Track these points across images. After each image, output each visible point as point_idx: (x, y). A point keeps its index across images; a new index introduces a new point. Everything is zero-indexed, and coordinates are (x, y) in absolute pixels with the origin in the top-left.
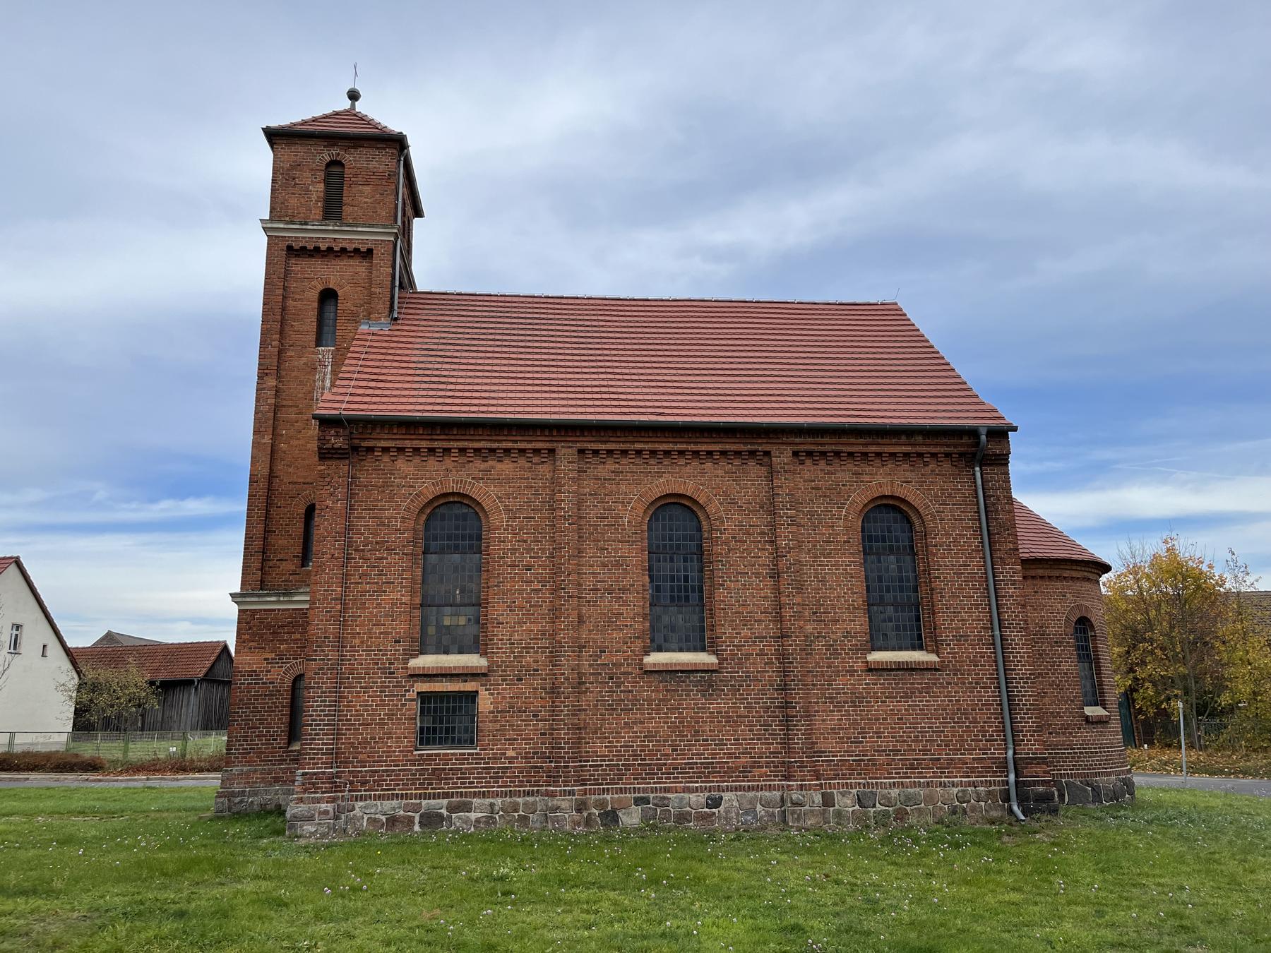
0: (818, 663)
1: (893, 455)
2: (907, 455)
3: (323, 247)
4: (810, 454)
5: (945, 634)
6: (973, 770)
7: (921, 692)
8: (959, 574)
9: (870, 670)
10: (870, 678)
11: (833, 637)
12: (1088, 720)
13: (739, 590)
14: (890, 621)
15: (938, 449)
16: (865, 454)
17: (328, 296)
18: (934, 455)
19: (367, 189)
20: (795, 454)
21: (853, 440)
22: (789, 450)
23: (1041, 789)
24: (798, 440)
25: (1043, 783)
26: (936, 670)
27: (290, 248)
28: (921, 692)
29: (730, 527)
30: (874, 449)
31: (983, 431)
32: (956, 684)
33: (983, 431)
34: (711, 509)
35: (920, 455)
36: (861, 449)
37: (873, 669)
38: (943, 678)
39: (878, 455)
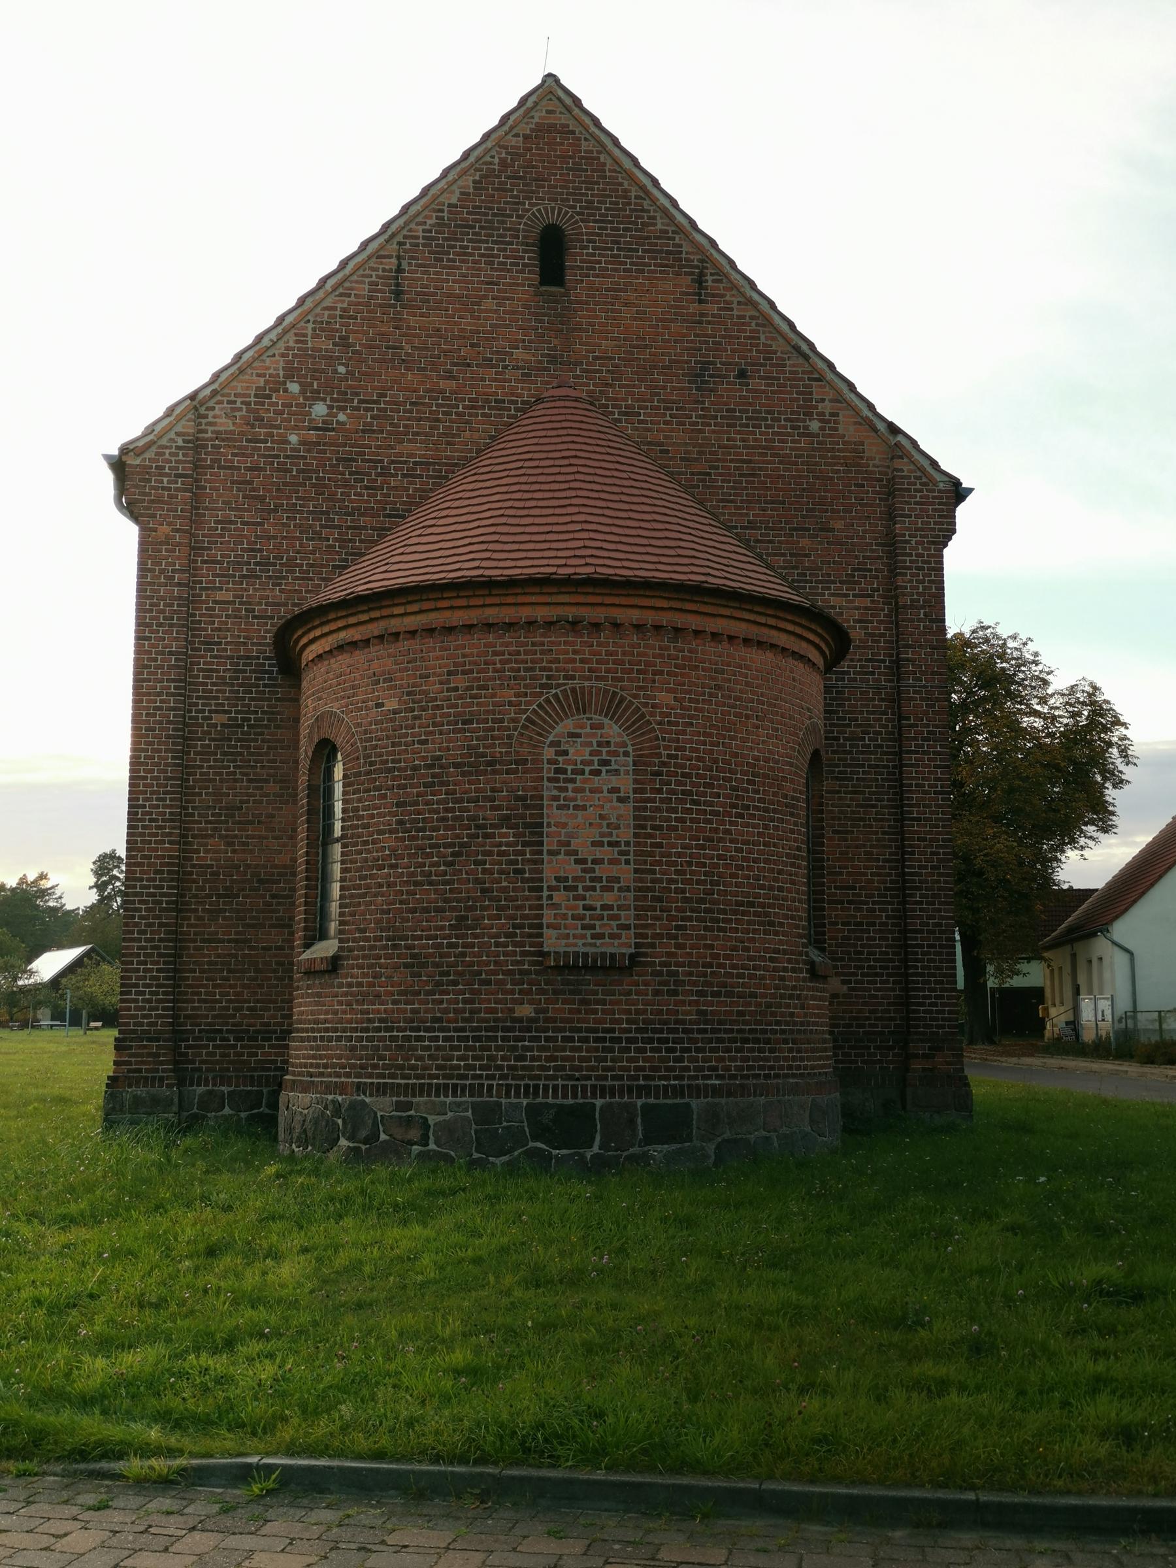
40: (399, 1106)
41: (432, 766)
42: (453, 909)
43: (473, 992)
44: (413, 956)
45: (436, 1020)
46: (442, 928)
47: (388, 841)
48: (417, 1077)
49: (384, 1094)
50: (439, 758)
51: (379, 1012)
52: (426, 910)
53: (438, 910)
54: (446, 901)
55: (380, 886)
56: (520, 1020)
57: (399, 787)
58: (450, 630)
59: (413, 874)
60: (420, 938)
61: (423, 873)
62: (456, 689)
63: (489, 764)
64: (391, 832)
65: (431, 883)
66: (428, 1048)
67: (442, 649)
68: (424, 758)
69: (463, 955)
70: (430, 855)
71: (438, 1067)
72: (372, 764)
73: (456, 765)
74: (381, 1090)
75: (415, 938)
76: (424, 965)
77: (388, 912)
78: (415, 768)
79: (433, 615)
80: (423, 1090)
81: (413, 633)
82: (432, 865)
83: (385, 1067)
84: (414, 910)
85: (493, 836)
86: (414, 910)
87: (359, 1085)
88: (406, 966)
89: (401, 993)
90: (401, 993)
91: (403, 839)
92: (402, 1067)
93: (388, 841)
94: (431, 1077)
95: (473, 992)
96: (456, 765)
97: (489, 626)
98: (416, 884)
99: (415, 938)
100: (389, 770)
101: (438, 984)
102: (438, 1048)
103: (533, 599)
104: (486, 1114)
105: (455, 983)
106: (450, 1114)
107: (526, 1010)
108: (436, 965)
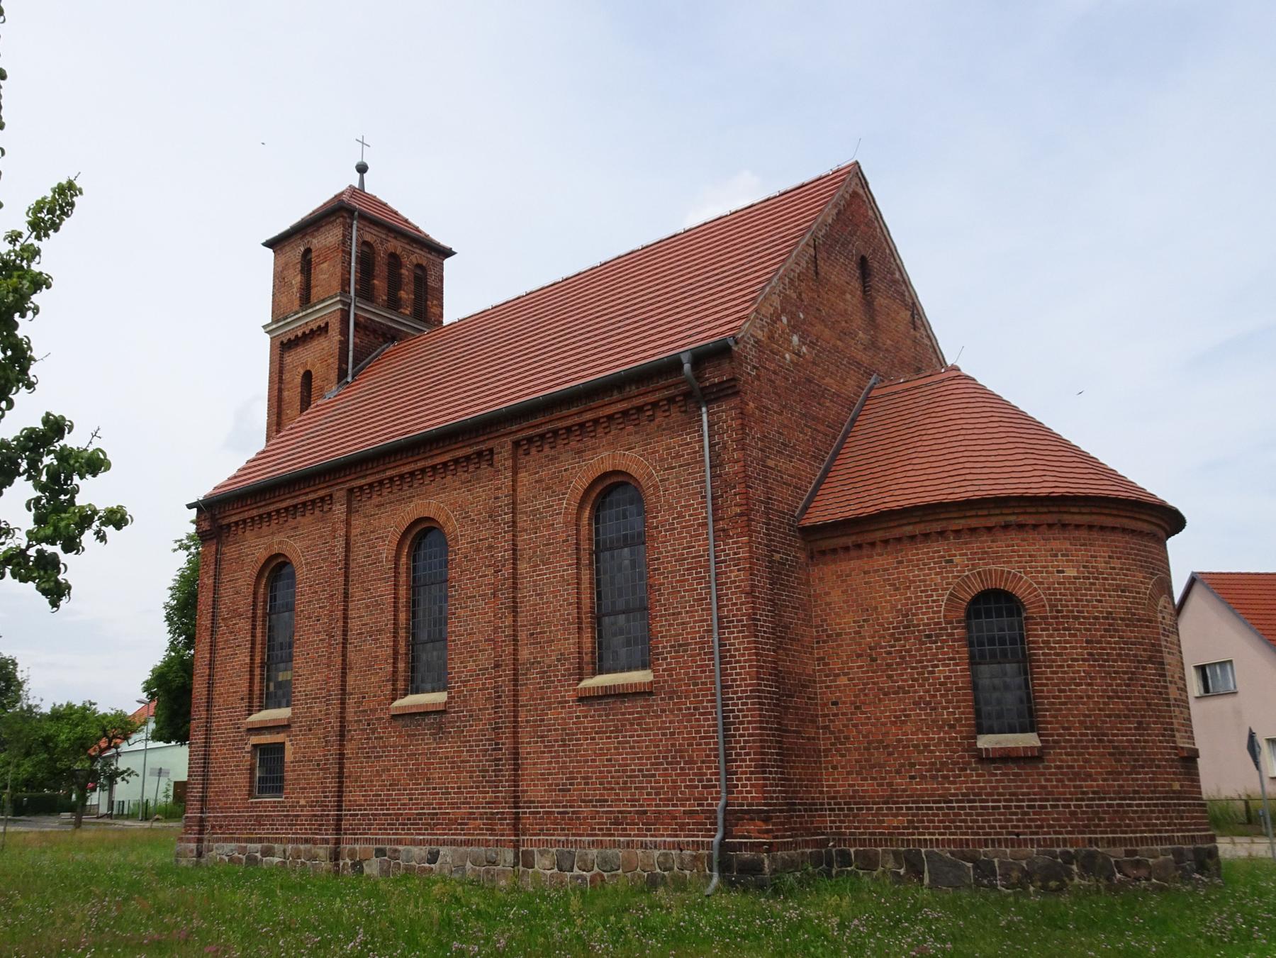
0: (532, 695)
1: (610, 418)
2: (625, 413)
3: (300, 334)
4: (530, 440)
5: (663, 645)
6: (682, 827)
7: (632, 724)
8: (681, 560)
9: (581, 699)
10: (580, 710)
11: (547, 661)
12: (986, 759)
13: (471, 617)
14: (621, 634)
15: (658, 396)
16: (582, 425)
17: (308, 376)
18: (655, 405)
19: (325, 265)
20: (517, 444)
21: (565, 412)
22: (508, 440)
23: (747, 855)
24: (514, 428)
25: (754, 846)
26: (651, 693)
27: (282, 343)
28: (632, 724)
29: (463, 545)
30: (588, 416)
31: (685, 358)
32: (672, 711)
33: (685, 358)
34: (448, 529)
35: (640, 409)
36: (577, 419)
37: (586, 699)
38: (657, 702)
39: (596, 421)
40: (1128, 853)
41: (1107, 618)
42: (1134, 716)
43: (1153, 773)
44: (1114, 748)
45: (1135, 792)
46: (1130, 729)
47: (1082, 667)
48: (1133, 832)
49: (1115, 845)
50: (1111, 613)
51: (1092, 786)
52: (1118, 716)
53: (1126, 716)
54: (1130, 710)
55: (1081, 697)
56: (1174, 792)
57: (1086, 630)
58: (1102, 528)
59: (1106, 691)
60: (1117, 735)
61: (1113, 691)
62: (1114, 568)
63: (1139, 620)
64: (1083, 660)
65: (1119, 697)
66: (1136, 812)
67: (1104, 540)
68: (1101, 612)
69: (1144, 747)
70: (1115, 679)
71: (1146, 825)
72: (1058, 611)
73: (1122, 619)
74: (1112, 842)
75: (1114, 735)
76: (1123, 754)
77: (1089, 716)
78: (1096, 618)
79: (1095, 517)
80: (1143, 841)
81: (1078, 526)
82: (1118, 685)
83: (1106, 826)
84: (1109, 716)
85: (1144, 668)
86: (1109, 716)
87: (1090, 839)
88: (1110, 754)
89: (1108, 773)
90: (1108, 773)
91: (1094, 666)
92: (1119, 826)
93: (1082, 667)
94: (1142, 832)
95: (1153, 773)
96: (1122, 619)
97: (1124, 530)
98: (1109, 697)
99: (1114, 735)
100: (1076, 618)
101: (1134, 767)
102: (1143, 812)
103: (1144, 517)
104: (1178, 854)
105: (1143, 767)
106: (1162, 858)
107: (1176, 786)
108: (1130, 754)
